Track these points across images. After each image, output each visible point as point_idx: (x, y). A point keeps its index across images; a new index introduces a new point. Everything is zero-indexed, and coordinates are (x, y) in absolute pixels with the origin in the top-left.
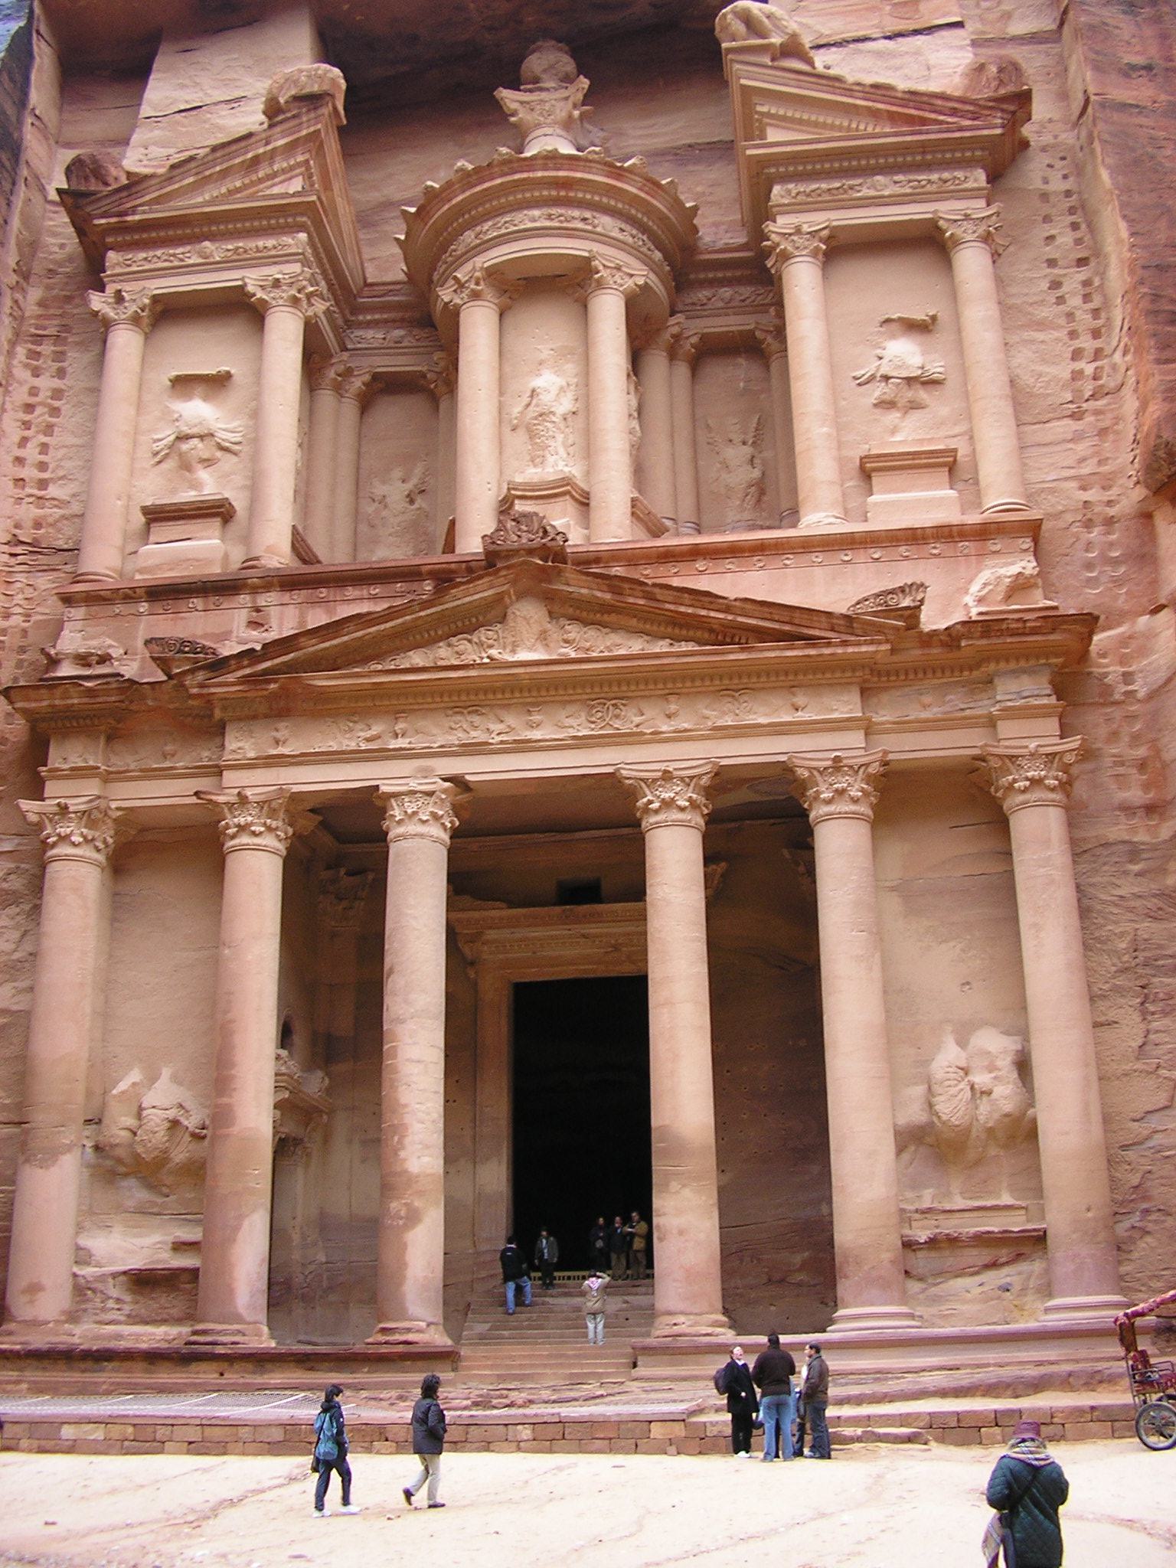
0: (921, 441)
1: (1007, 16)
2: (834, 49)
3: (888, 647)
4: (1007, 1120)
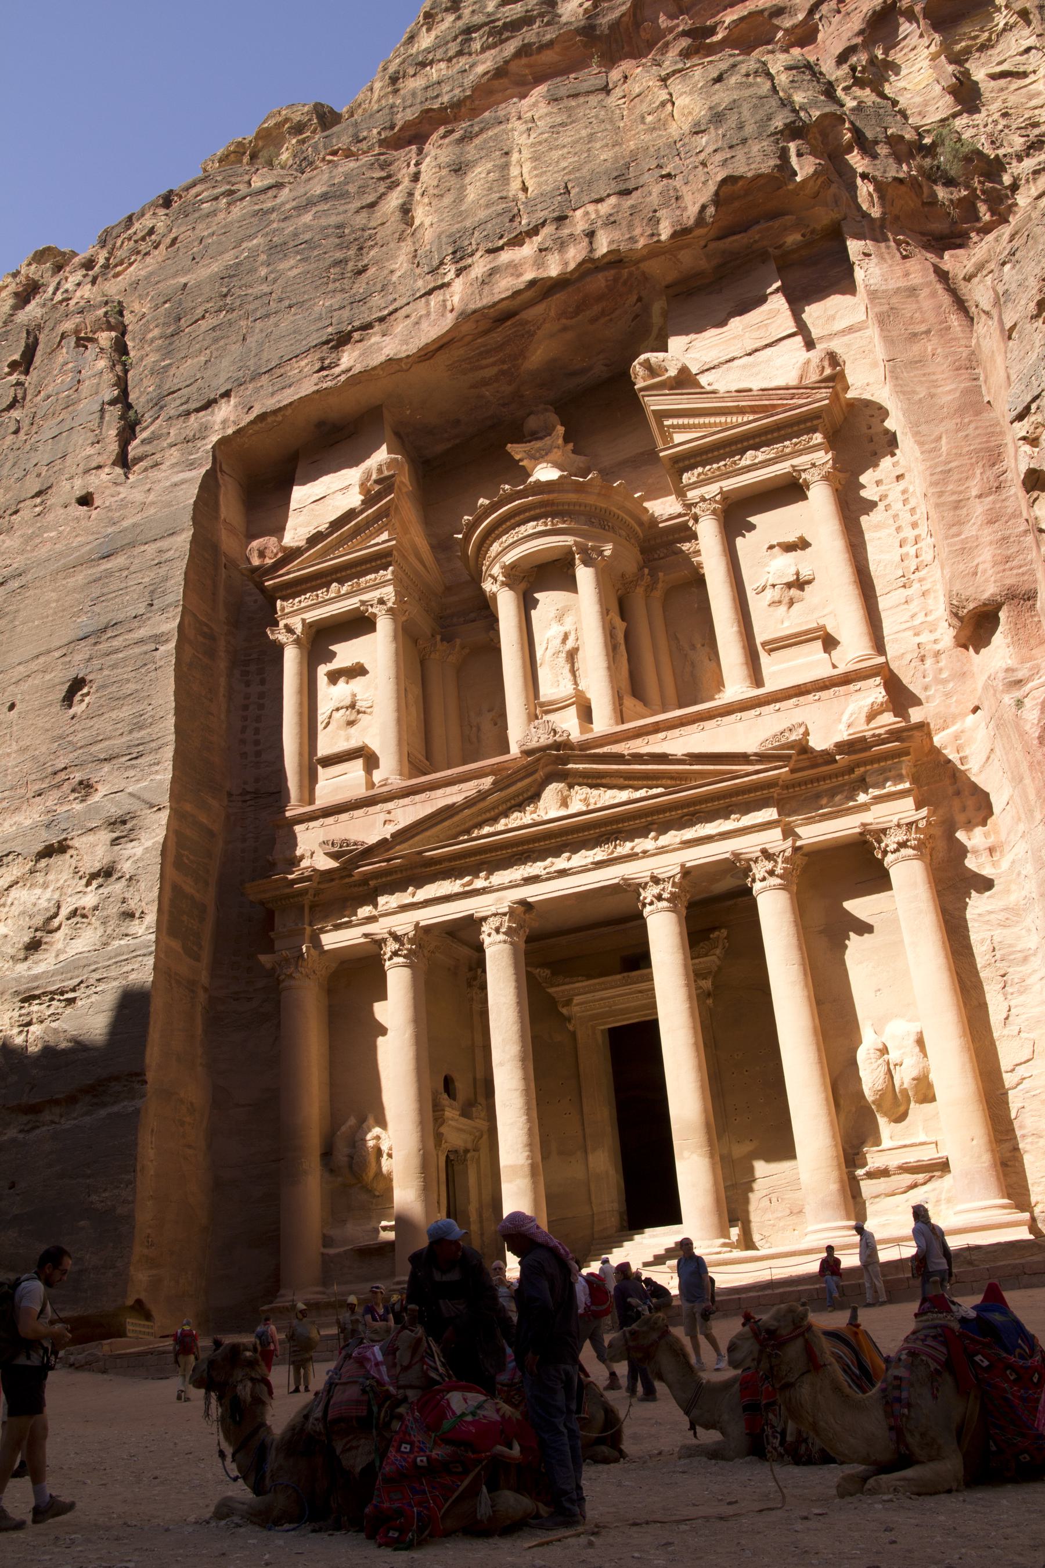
1: (833, 318)
2: (713, 371)
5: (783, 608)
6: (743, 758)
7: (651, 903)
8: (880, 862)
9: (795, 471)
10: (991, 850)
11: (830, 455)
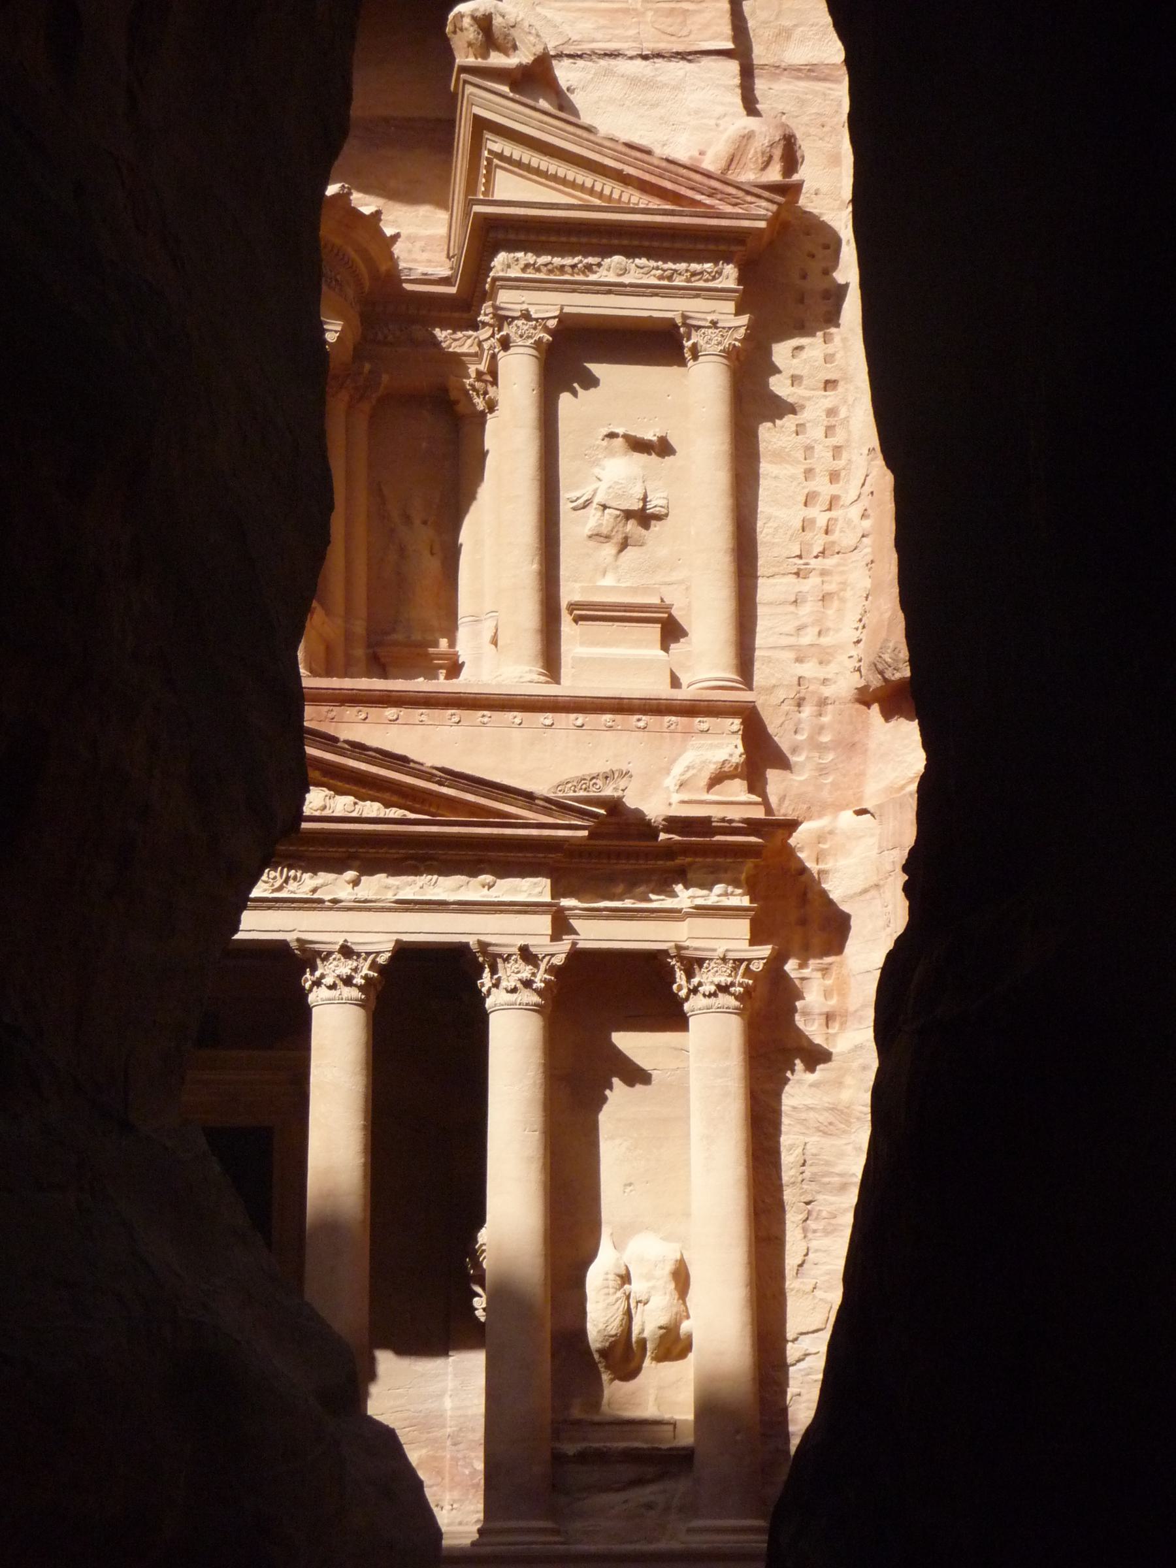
0: (634, 590)
2: (581, 63)
3: (585, 833)
4: (662, 1331)
5: (609, 550)
6: (528, 798)
7: (333, 987)
8: (678, 1003)
9: (684, 324)
10: (829, 1018)
11: (744, 319)
